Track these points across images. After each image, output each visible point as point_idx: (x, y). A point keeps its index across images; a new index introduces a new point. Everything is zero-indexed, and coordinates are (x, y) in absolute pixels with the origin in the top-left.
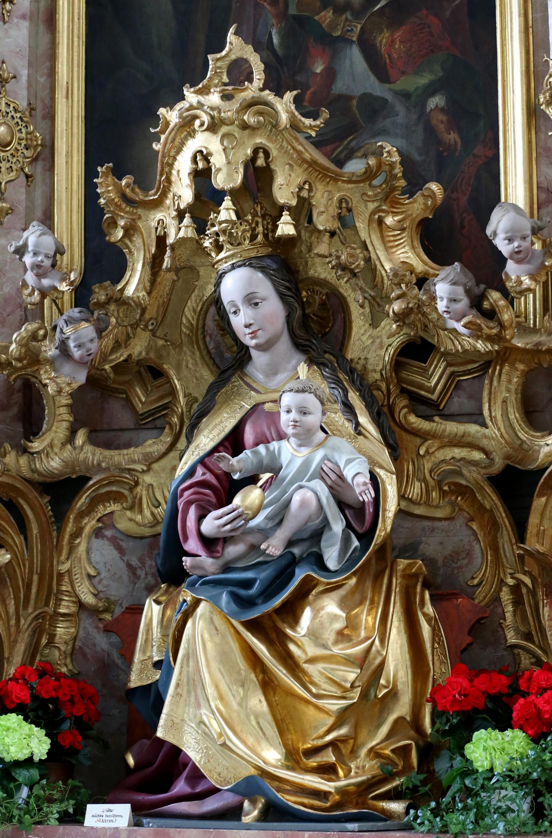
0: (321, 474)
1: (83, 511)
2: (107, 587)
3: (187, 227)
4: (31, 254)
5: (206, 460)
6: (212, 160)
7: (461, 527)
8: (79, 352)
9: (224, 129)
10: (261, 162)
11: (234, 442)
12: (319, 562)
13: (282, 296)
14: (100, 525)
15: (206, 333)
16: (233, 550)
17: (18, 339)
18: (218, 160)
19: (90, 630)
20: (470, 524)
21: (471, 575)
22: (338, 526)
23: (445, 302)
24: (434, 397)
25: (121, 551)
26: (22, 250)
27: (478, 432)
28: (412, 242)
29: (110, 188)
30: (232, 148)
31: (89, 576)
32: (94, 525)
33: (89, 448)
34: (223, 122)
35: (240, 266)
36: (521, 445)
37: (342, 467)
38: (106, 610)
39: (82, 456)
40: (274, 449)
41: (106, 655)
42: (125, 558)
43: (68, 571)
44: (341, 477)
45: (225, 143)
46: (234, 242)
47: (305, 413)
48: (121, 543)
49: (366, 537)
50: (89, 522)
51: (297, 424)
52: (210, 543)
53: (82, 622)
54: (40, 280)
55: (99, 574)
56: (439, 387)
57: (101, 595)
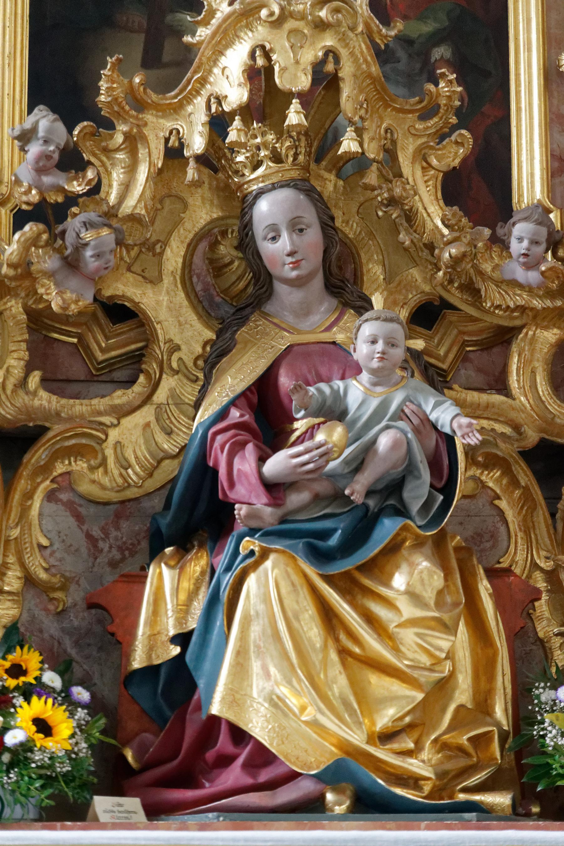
1: (41, 466)
2: (60, 561)
3: (239, 130)
4: (41, 142)
5: (237, 402)
6: (274, 57)
7: (483, 506)
8: (96, 263)
9: (290, 24)
10: (330, 67)
14: (55, 486)
15: (192, 273)
16: (296, 499)
17: (22, 239)
19: (36, 612)
20: (497, 502)
21: (496, 559)
23: (525, 243)
24: (445, 367)
25: (79, 518)
26: (29, 136)
27: (503, 403)
28: (436, 192)
29: (115, 85)
30: (301, 47)
31: (41, 547)
32: (48, 486)
33: (43, 394)
35: (282, 187)
36: (553, 419)
37: (428, 410)
38: (63, 588)
39: (37, 403)
40: (339, 388)
41: (56, 644)
42: (85, 528)
43: (16, 539)
45: (292, 40)
46: (277, 158)
47: (393, 345)
48: (80, 509)
50: (42, 482)
51: (385, 357)
52: (274, 489)
53: (26, 602)
54: (40, 176)
55: (51, 545)
56: (451, 356)
57: (53, 570)
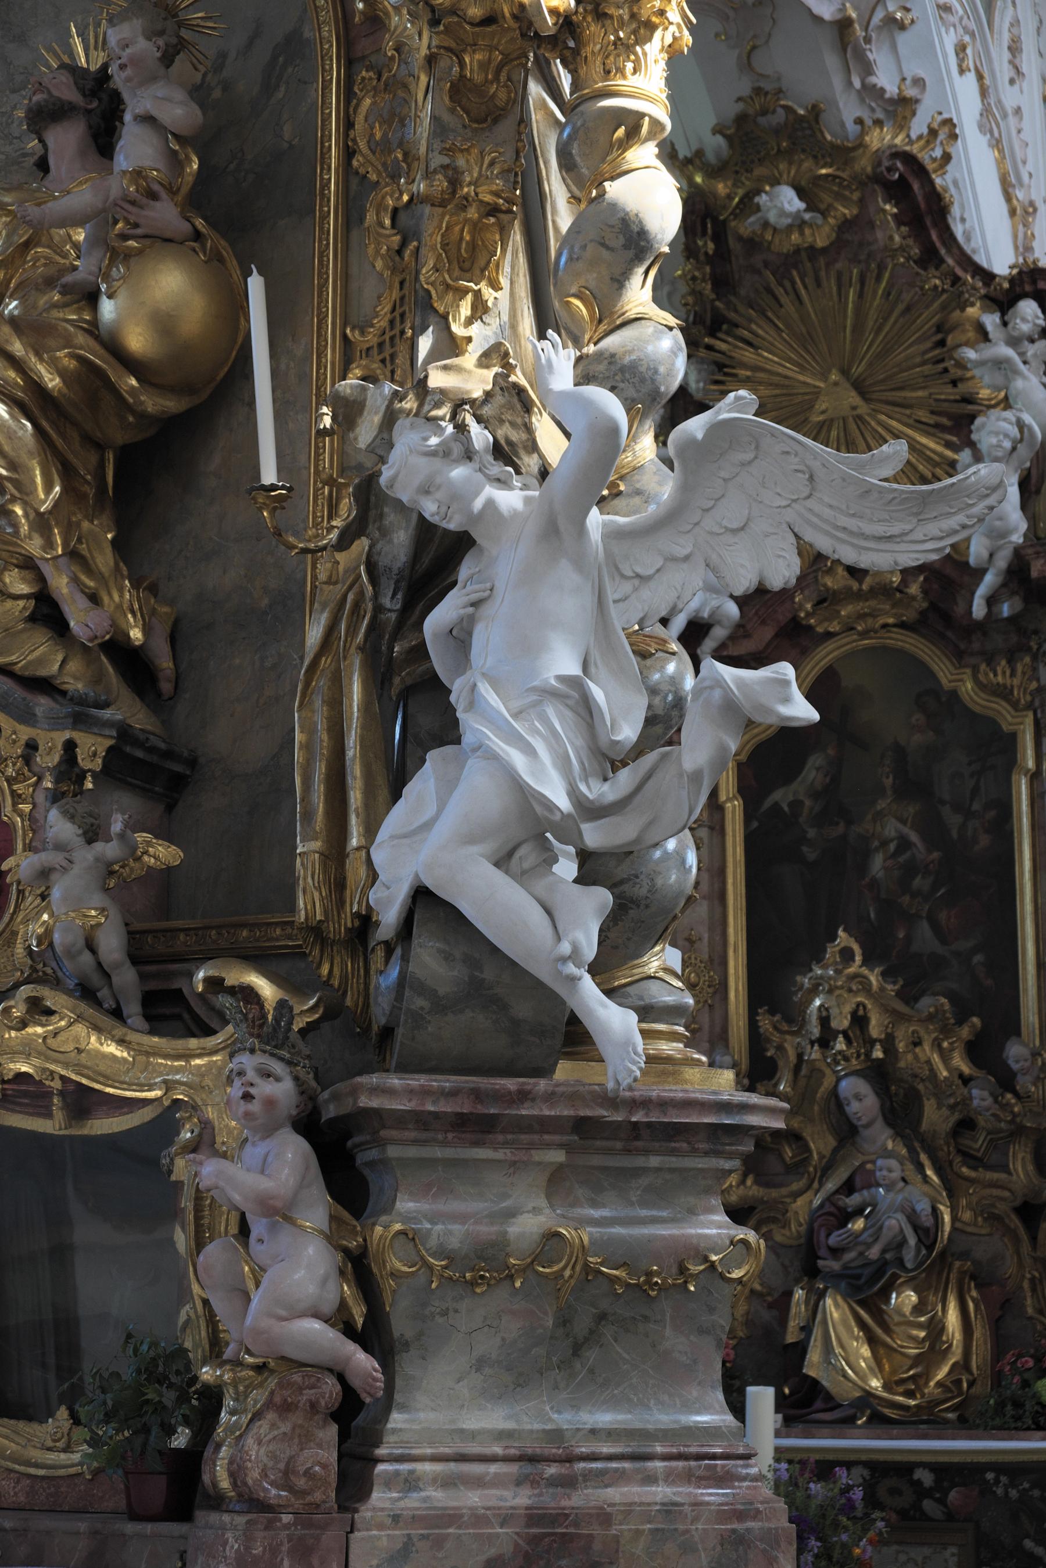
0: (902, 1209)
9: (838, 992)
10: (861, 1012)
11: (849, 1187)
12: (900, 1262)
13: (877, 1094)
18: (834, 1012)
22: (912, 1241)
24: (979, 1155)
33: (755, 1187)
34: (837, 988)
38: (769, 1294)
44: (914, 1210)
46: (846, 1059)
49: (930, 1248)
52: (836, 1252)
